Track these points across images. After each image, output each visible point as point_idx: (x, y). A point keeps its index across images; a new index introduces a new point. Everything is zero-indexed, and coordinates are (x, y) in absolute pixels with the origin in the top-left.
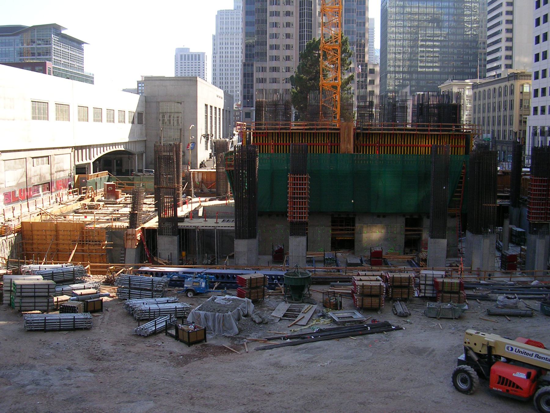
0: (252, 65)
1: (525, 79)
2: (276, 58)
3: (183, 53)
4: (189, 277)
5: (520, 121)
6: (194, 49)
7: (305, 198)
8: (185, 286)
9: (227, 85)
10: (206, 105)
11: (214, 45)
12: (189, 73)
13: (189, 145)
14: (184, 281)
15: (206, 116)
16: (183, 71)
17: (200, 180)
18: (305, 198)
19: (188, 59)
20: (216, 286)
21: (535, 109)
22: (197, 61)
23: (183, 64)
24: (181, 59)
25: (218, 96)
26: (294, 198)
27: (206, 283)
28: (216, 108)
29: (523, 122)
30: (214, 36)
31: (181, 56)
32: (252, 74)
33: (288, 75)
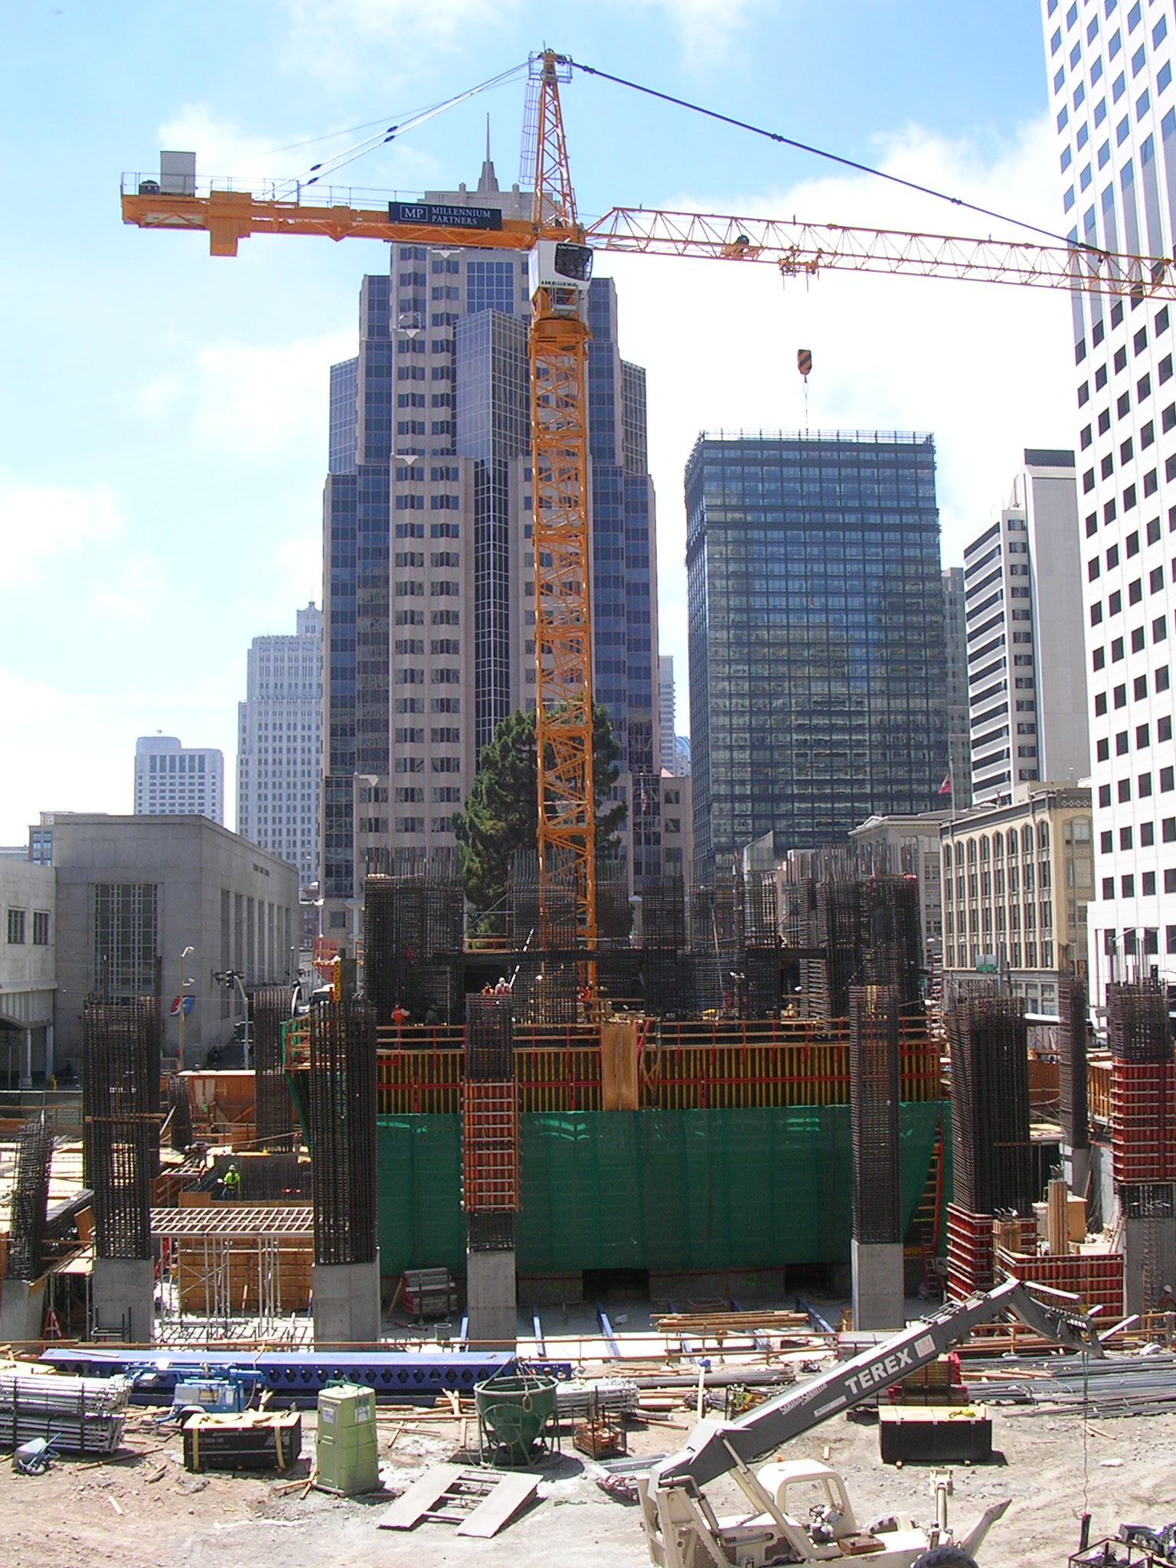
0: (349, 784)
1: (1075, 806)
2: (414, 765)
3: (158, 752)
4: (190, 1376)
5: (1071, 918)
6: (191, 742)
7: (509, 1145)
8: (177, 1401)
9: (292, 838)
10: (225, 893)
11: (243, 729)
12: (174, 805)
13: (177, 1002)
14: (172, 1390)
15: (225, 921)
16: (158, 801)
17: (210, 1096)
18: (509, 1145)
19: (172, 769)
20: (264, 1400)
21: (1108, 883)
22: (197, 774)
23: (158, 781)
24: (153, 769)
25: (256, 868)
26: (480, 1145)
27: (237, 1391)
28: (250, 900)
29: (1078, 917)
30: (242, 707)
31: (153, 758)
32: (349, 807)
33: (446, 810)
